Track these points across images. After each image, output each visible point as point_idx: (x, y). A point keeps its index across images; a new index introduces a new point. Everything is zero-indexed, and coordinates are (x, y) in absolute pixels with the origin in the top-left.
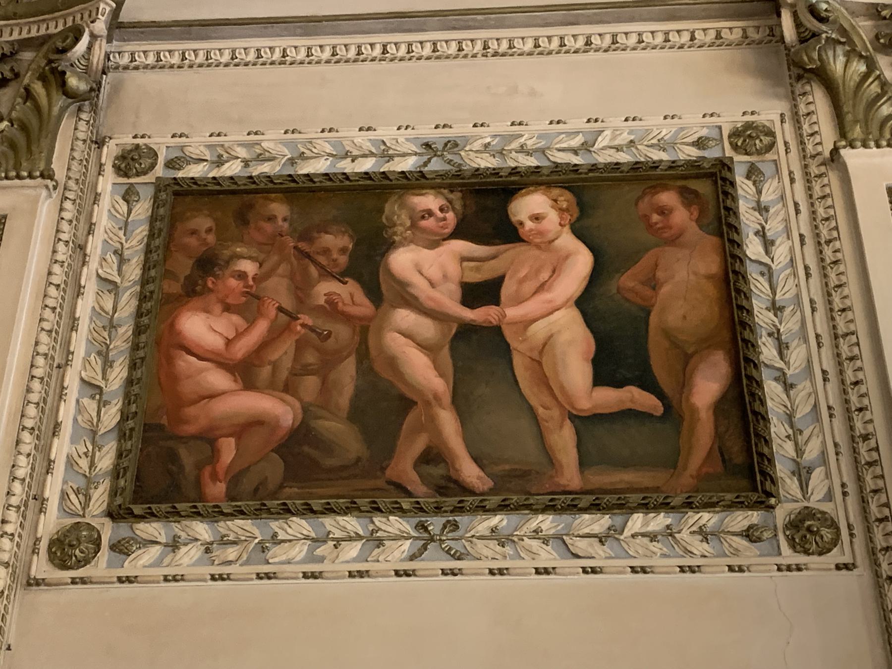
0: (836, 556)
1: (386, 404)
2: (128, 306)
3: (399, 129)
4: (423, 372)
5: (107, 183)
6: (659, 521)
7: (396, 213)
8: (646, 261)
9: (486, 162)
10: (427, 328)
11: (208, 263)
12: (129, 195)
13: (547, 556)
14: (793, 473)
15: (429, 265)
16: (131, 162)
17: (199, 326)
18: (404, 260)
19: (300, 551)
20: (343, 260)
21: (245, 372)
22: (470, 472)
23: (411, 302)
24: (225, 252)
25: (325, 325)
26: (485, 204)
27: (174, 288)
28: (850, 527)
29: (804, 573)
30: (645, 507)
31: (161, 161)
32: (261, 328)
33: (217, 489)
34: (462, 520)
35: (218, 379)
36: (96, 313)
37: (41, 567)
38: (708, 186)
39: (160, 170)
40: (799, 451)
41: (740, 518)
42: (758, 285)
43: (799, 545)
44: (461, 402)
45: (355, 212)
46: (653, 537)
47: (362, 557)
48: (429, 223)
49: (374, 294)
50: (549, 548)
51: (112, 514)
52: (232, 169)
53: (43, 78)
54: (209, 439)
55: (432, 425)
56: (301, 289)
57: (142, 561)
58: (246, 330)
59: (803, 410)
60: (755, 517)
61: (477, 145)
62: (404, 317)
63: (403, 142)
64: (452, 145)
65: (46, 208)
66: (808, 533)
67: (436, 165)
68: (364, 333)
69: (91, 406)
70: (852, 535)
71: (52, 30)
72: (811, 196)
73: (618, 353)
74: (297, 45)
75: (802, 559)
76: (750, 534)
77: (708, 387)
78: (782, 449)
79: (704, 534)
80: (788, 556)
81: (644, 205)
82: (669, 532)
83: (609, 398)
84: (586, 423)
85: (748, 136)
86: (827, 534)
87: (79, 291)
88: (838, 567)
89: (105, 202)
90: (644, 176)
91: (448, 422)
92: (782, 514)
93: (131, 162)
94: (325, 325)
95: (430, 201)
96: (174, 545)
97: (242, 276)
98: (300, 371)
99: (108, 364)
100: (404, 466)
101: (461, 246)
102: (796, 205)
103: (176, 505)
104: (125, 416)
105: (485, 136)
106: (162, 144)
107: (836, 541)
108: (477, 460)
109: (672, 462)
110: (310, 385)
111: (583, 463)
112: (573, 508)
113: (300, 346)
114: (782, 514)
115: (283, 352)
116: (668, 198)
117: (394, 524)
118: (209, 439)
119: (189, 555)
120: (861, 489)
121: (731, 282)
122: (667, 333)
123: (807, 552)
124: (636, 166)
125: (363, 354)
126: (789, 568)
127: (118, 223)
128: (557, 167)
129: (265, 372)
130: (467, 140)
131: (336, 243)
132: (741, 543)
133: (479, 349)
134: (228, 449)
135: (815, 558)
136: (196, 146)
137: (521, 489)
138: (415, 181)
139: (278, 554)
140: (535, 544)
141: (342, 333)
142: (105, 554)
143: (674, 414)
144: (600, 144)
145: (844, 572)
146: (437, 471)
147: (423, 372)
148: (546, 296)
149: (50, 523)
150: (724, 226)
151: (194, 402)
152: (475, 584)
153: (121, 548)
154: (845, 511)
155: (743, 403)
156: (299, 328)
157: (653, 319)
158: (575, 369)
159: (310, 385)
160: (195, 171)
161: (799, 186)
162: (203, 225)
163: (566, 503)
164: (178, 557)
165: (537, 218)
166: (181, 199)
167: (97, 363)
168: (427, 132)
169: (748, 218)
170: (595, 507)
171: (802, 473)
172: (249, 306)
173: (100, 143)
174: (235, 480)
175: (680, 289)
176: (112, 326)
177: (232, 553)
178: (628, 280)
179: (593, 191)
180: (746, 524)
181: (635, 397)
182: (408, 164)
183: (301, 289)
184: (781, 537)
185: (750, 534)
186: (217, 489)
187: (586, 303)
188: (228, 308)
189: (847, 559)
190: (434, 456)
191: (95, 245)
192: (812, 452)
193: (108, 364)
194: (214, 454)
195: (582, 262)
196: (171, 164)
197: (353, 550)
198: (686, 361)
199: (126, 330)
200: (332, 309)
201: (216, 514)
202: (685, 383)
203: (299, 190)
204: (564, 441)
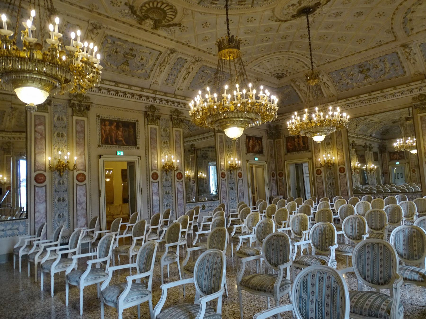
1: (295, 147)
4: (297, 145)
15: (296, 140)
21: (290, 146)
66: (310, 151)
73: (304, 144)
93: (284, 136)
127: (284, 139)
133: (299, 144)
137: (301, 150)
147: (297, 145)
158: (302, 144)
163: (302, 151)
164: (290, 155)
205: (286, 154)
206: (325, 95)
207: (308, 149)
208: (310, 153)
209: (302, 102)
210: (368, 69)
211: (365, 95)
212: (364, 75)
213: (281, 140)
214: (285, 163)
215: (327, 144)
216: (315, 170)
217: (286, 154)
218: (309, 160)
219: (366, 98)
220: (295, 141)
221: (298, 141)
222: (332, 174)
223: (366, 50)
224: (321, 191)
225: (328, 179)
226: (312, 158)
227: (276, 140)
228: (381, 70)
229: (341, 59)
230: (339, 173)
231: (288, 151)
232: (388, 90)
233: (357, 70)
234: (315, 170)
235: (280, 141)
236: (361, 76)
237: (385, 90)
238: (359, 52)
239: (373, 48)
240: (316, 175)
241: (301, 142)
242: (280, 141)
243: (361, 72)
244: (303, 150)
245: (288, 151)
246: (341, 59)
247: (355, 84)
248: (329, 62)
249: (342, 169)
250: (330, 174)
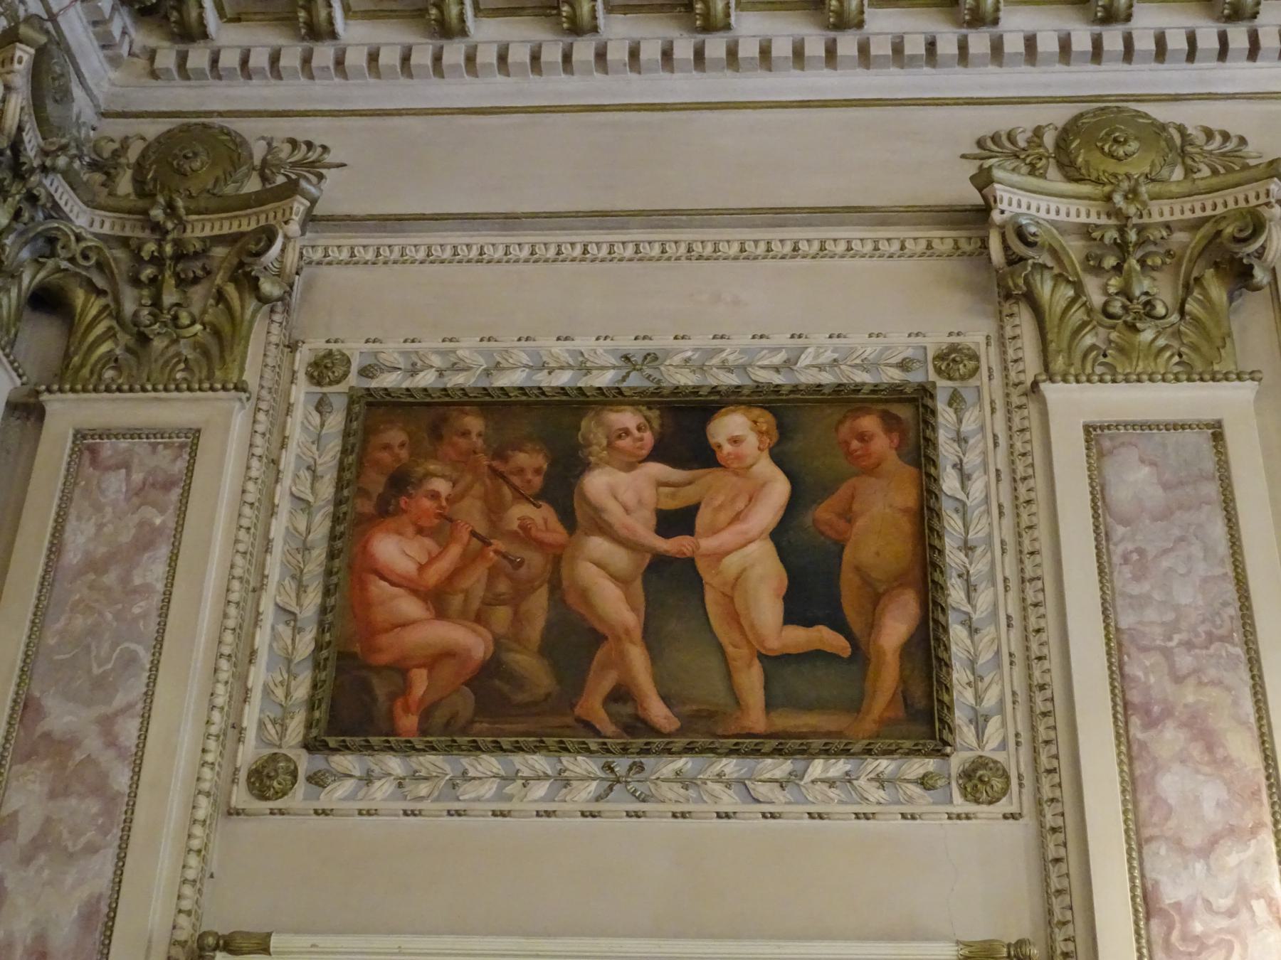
0: (1004, 806)
1: (576, 639)
2: (321, 526)
3: (598, 339)
4: (616, 605)
5: (301, 392)
6: (839, 767)
7: (593, 430)
8: (844, 490)
9: (686, 379)
10: (620, 558)
11: (400, 482)
12: (321, 406)
13: (729, 800)
14: (971, 721)
15: (624, 489)
16: (324, 369)
17: (394, 549)
18: (599, 484)
19: (489, 789)
20: (538, 481)
21: (437, 600)
22: (658, 712)
23: (602, 528)
24: (418, 469)
25: (517, 551)
26: (683, 427)
27: (367, 507)
28: (1020, 777)
29: (974, 821)
30: (826, 752)
31: (354, 368)
32: (455, 551)
33: (409, 722)
34: (648, 761)
35: (410, 607)
36: (291, 532)
37: (241, 796)
38: (908, 413)
39: (353, 380)
40: (978, 698)
41: (916, 766)
42: (952, 523)
43: (972, 795)
44: (652, 637)
45: (547, 429)
46: (831, 783)
47: (549, 798)
48: (625, 443)
49: (568, 518)
50: (731, 792)
51: (312, 746)
52: (426, 379)
53: (233, 279)
54: (401, 670)
55: (621, 661)
56: (494, 510)
57: (338, 792)
58: (440, 553)
59: (985, 657)
60: (931, 764)
61: (677, 360)
62: (598, 545)
63: (602, 353)
64: (652, 358)
65: (239, 421)
66: (980, 781)
67: (635, 381)
68: (557, 559)
69: (285, 632)
70: (1021, 785)
71: (245, 228)
72: (1010, 428)
73: (810, 594)
74: (493, 241)
75: (971, 808)
76: (924, 782)
77: (895, 629)
78: (963, 696)
79: (880, 781)
80: (960, 804)
81: (845, 429)
82: (848, 778)
83: (799, 638)
84: (775, 664)
85: (953, 360)
86: (997, 783)
87: (272, 511)
88: (1005, 817)
89: (298, 413)
90: (846, 399)
91: (637, 657)
92: (957, 762)
93: (324, 369)
94: (517, 551)
95: (627, 418)
96: (368, 779)
97: (435, 496)
98: (493, 601)
99: (301, 589)
100: (593, 705)
101: (657, 469)
102: (995, 436)
103: (370, 739)
104: (319, 647)
105: (687, 349)
106: (356, 350)
107: (1005, 791)
108: (666, 699)
109: (856, 706)
110: (502, 615)
111: (769, 706)
112: (756, 752)
113: (493, 573)
114: (957, 762)
115: (475, 580)
116: (869, 423)
117: (581, 765)
118: (401, 670)
119: (383, 789)
120: (1034, 739)
121: (926, 518)
122: (858, 569)
123: (977, 801)
124: (839, 388)
125: (555, 586)
126: (959, 817)
127: (313, 437)
128: (758, 388)
129: (456, 601)
130: (668, 353)
131: (530, 461)
132: (915, 790)
133: (672, 583)
134: (420, 681)
135: (984, 808)
136: (391, 352)
137: (708, 730)
138: (613, 398)
139: (468, 791)
140: (717, 788)
141: (535, 561)
142: (301, 787)
143: (860, 657)
144: (805, 360)
145: (1011, 821)
146: (627, 709)
147: (616, 605)
148: (739, 527)
149: (249, 753)
150: (921, 456)
151: (387, 631)
152: (658, 827)
153: (317, 780)
154: (1017, 762)
155: (927, 648)
156: (492, 554)
157: (847, 554)
158: (766, 608)
159: (502, 615)
160: (389, 381)
161: (1000, 414)
162: (397, 440)
163: (750, 745)
164: (374, 792)
165: (735, 441)
166: (375, 410)
167: (290, 585)
168: (627, 344)
169: (946, 449)
170: (778, 752)
171: (979, 721)
172: (440, 528)
173: (293, 347)
174: (426, 714)
175: (874, 528)
176: (306, 548)
177: (423, 789)
178: (824, 512)
179: (791, 413)
180: (922, 771)
181: (825, 637)
182: (604, 379)
183: (494, 510)
184: (954, 785)
185: (924, 782)
186: (409, 722)
187: (780, 535)
188: (420, 531)
189: (1014, 809)
190: (621, 695)
191: (288, 461)
192: (990, 700)
193: (301, 589)
194: (406, 688)
195: (780, 489)
196: (365, 372)
197: (540, 789)
198: (876, 600)
199: (319, 554)
200: (525, 535)
201: (408, 749)
202: (873, 625)
203: (496, 405)
204: (752, 681)
205: (266, 780)
207: (923, 718)
213: (227, 424)
217: (266, 780)
221: (676, 521)
231: (356, 703)
235: (191, 440)
241: (744, 555)
242: (191, 440)
245: (356, 703)
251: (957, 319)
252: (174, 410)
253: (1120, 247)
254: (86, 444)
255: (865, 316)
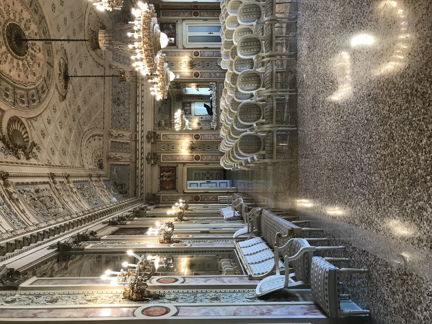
1: (171, 180)
11: (164, 188)
26: (162, 176)
45: (162, 182)
65: (162, 195)
66: (177, 165)
85: (159, 165)
93: (158, 192)
121: (166, 167)
133: (169, 177)
137: (175, 175)
150: (163, 167)
155: (172, 167)
164: (178, 187)
175: (167, 169)
179: (161, 172)
205: (177, 191)
206: (129, 142)
208: (179, 165)
209: (129, 165)
210: (118, 99)
211: (138, 108)
212: (122, 104)
214: (185, 193)
215: (173, 149)
216: (195, 161)
218: (186, 167)
219: (140, 109)
220: (166, 180)
221: (166, 177)
222: (200, 146)
223: (104, 88)
224: (214, 157)
225: (204, 150)
226: (184, 164)
227: (161, 202)
228: (122, 92)
229: (104, 108)
230: (199, 140)
232: (138, 92)
233: (116, 106)
234: (195, 161)
236: (121, 106)
237: (138, 94)
238: (104, 93)
239: (104, 83)
240: (199, 161)
241: (167, 174)
243: (118, 105)
244: (176, 172)
246: (104, 108)
247: (126, 114)
248: (104, 118)
249: (196, 137)
250: (200, 148)
251: (157, 165)
252: (161, 197)
253: (154, 159)
254: (163, 201)
255: (156, 169)
